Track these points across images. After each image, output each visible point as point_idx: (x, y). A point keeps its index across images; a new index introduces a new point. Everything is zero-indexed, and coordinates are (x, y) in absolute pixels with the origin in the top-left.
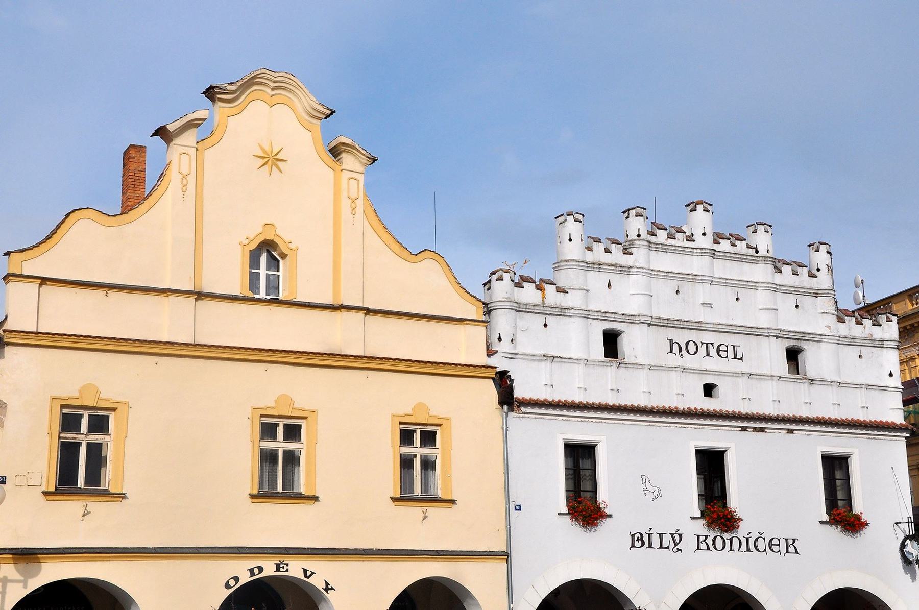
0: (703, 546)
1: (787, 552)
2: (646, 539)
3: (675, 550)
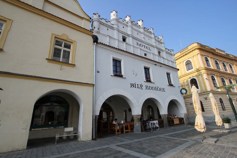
0: (147, 88)
2: (134, 85)
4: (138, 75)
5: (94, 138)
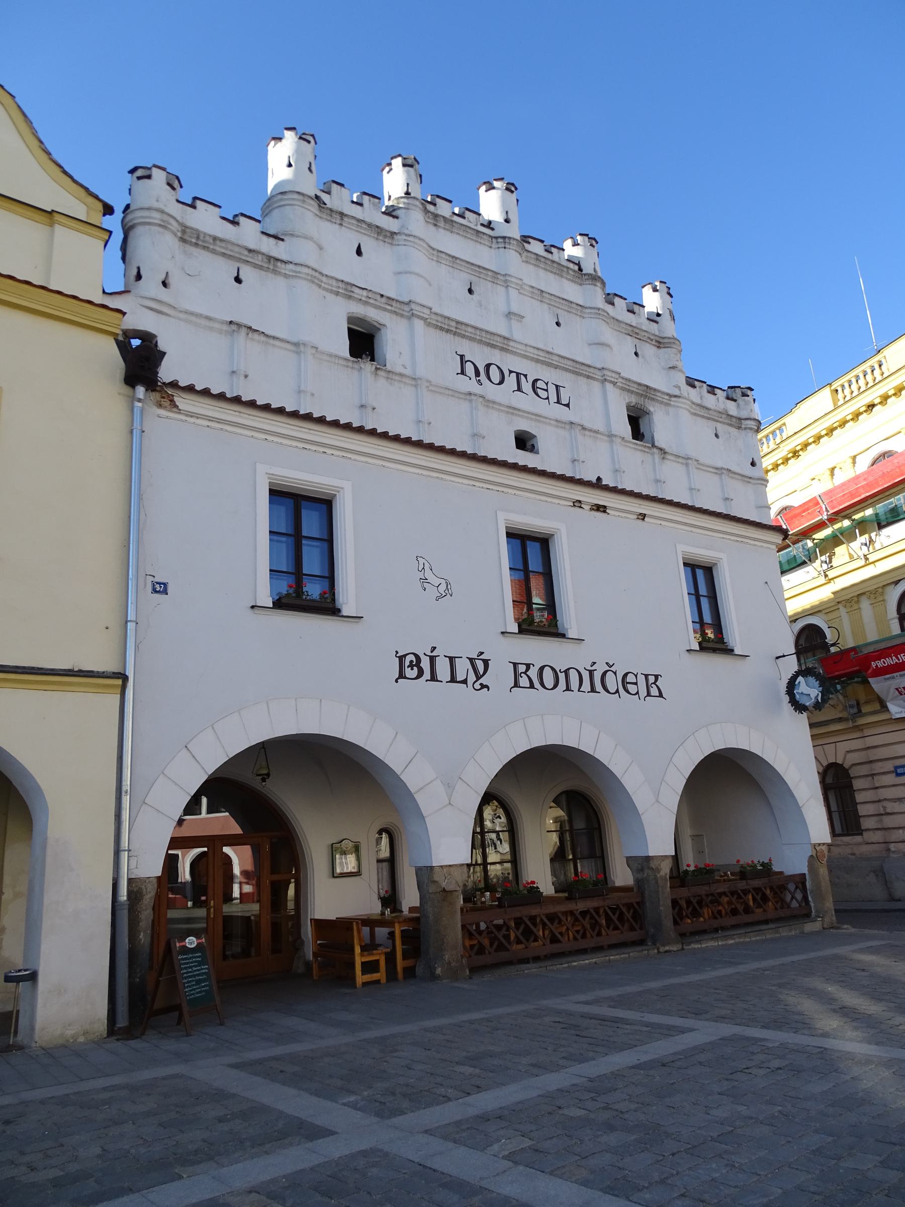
0: (524, 681)
1: (649, 695)
2: (425, 664)
3: (477, 686)
4: (454, 588)
5: (122, 1022)
